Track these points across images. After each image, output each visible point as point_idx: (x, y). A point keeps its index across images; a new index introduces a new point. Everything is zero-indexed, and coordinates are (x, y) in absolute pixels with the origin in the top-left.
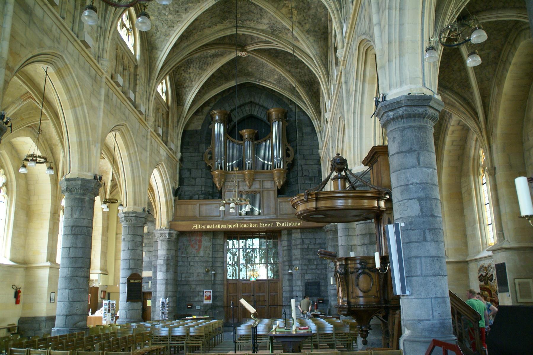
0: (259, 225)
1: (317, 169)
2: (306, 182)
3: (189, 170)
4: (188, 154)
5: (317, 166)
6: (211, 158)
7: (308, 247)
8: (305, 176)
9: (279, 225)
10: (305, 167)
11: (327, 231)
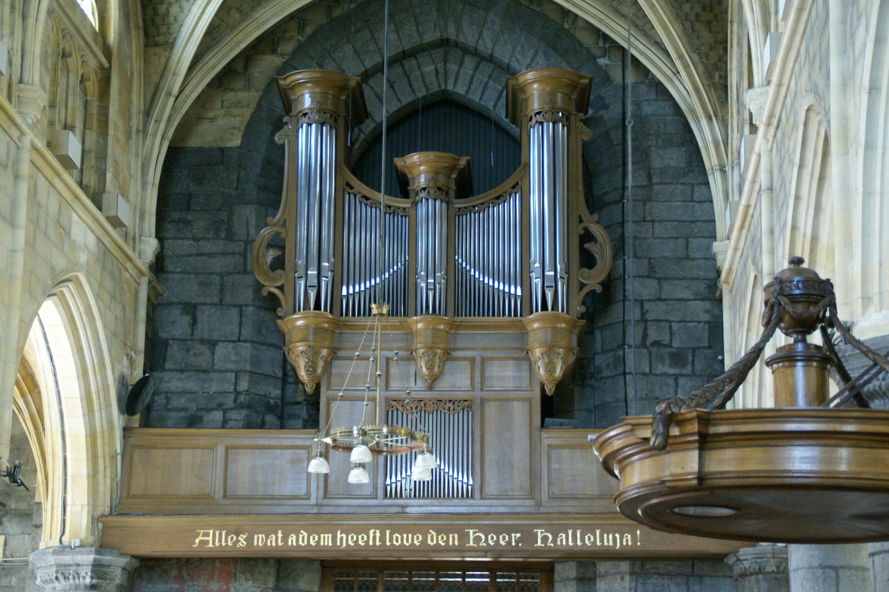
0: (464, 537)
1: (707, 317)
2: (660, 369)
3: (190, 309)
4: (186, 245)
5: (707, 305)
6: (279, 264)
8: (656, 343)
9: (545, 539)
10: (655, 311)
11: (744, 575)
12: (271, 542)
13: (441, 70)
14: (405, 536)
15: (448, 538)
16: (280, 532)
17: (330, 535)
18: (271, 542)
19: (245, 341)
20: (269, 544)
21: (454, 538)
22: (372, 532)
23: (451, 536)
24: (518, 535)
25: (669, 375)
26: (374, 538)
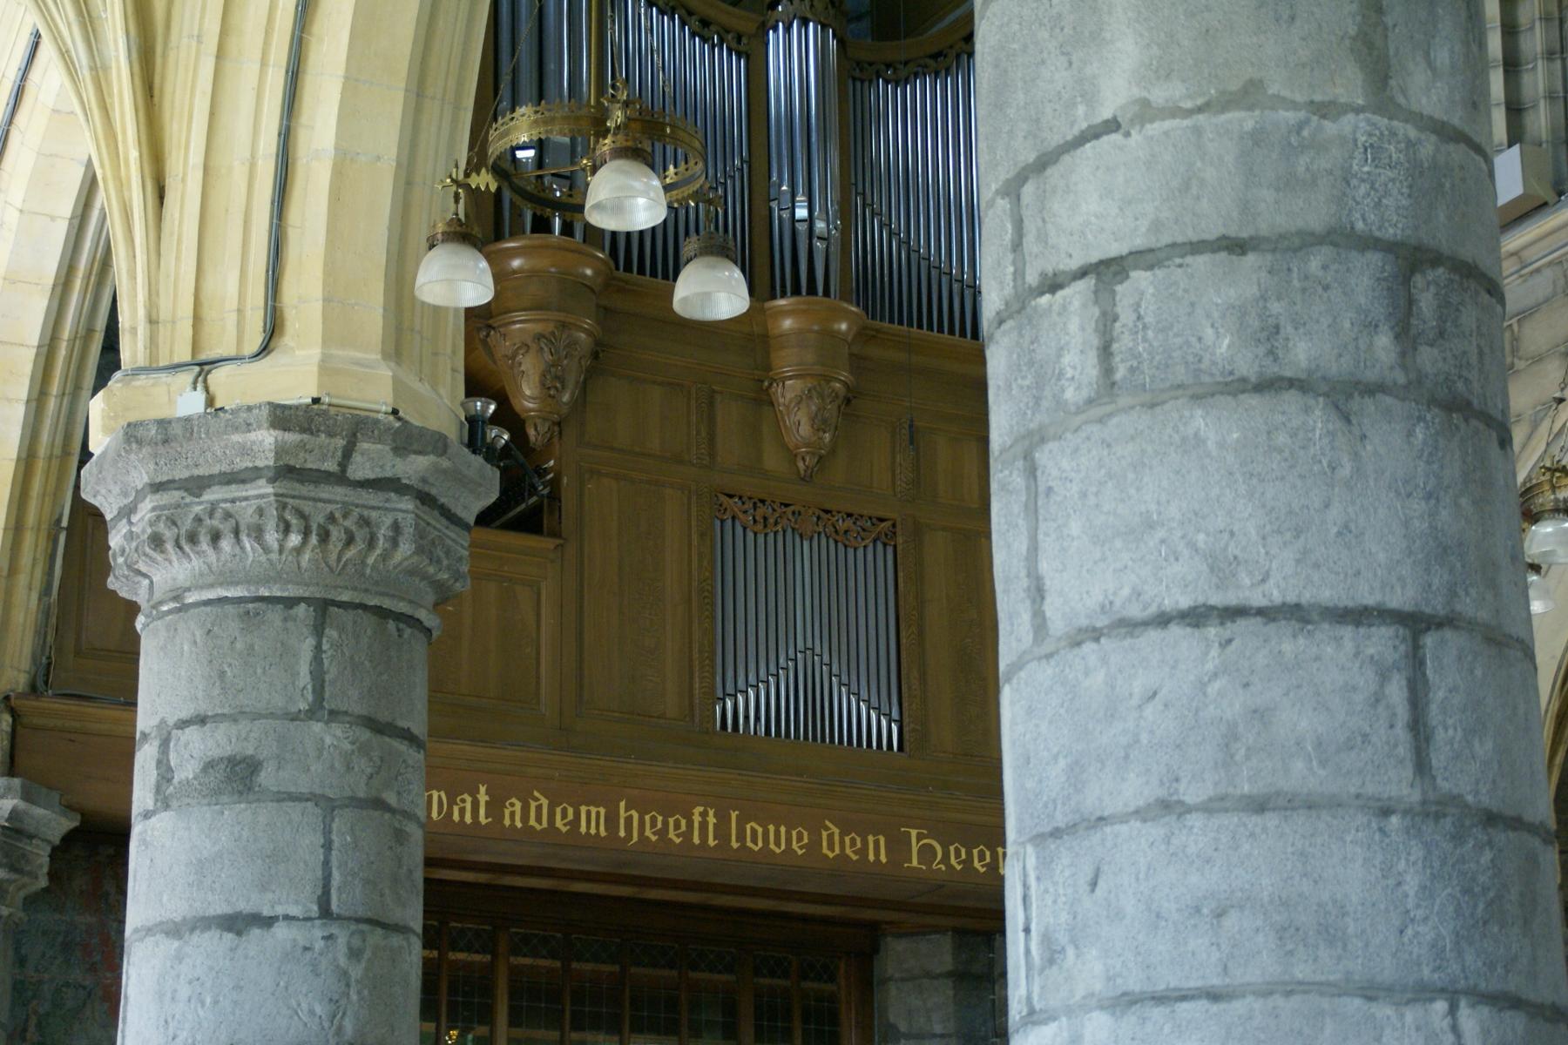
0: (898, 845)
12: (462, 811)
14: (771, 828)
16: (483, 789)
17: (602, 811)
18: (462, 811)
20: (456, 817)
21: (877, 843)
23: (871, 839)
26: (704, 826)
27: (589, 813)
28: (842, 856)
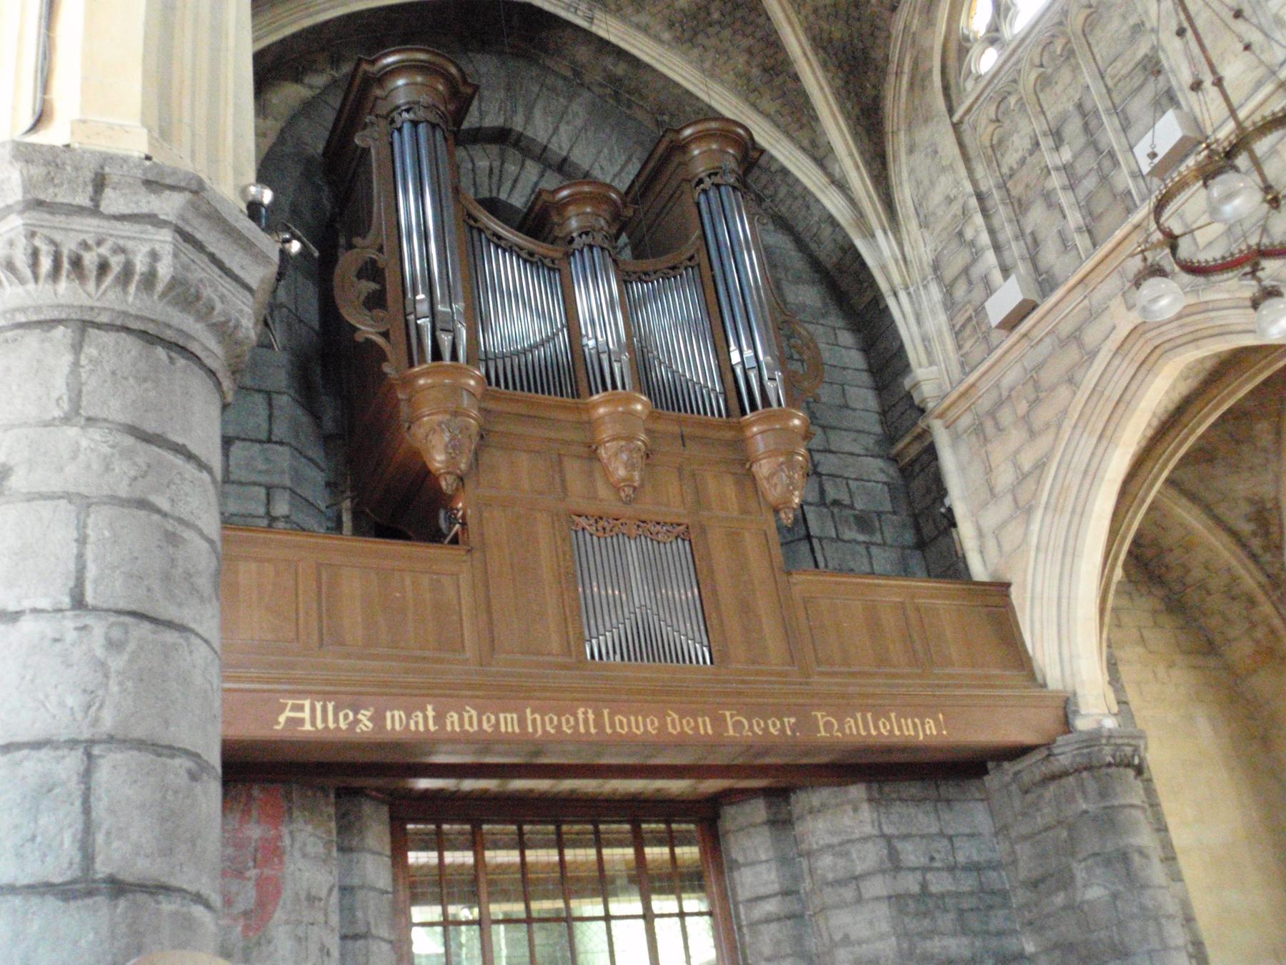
0: (718, 722)
7: (924, 885)
9: (828, 725)
12: (417, 723)
13: (496, 171)
14: (633, 719)
15: (696, 722)
16: (430, 708)
17: (515, 716)
18: (417, 723)
19: (281, 443)
20: (413, 727)
21: (704, 723)
22: (580, 711)
23: (700, 720)
24: (793, 720)
25: (858, 543)
26: (586, 721)
27: (506, 718)
28: (682, 733)
